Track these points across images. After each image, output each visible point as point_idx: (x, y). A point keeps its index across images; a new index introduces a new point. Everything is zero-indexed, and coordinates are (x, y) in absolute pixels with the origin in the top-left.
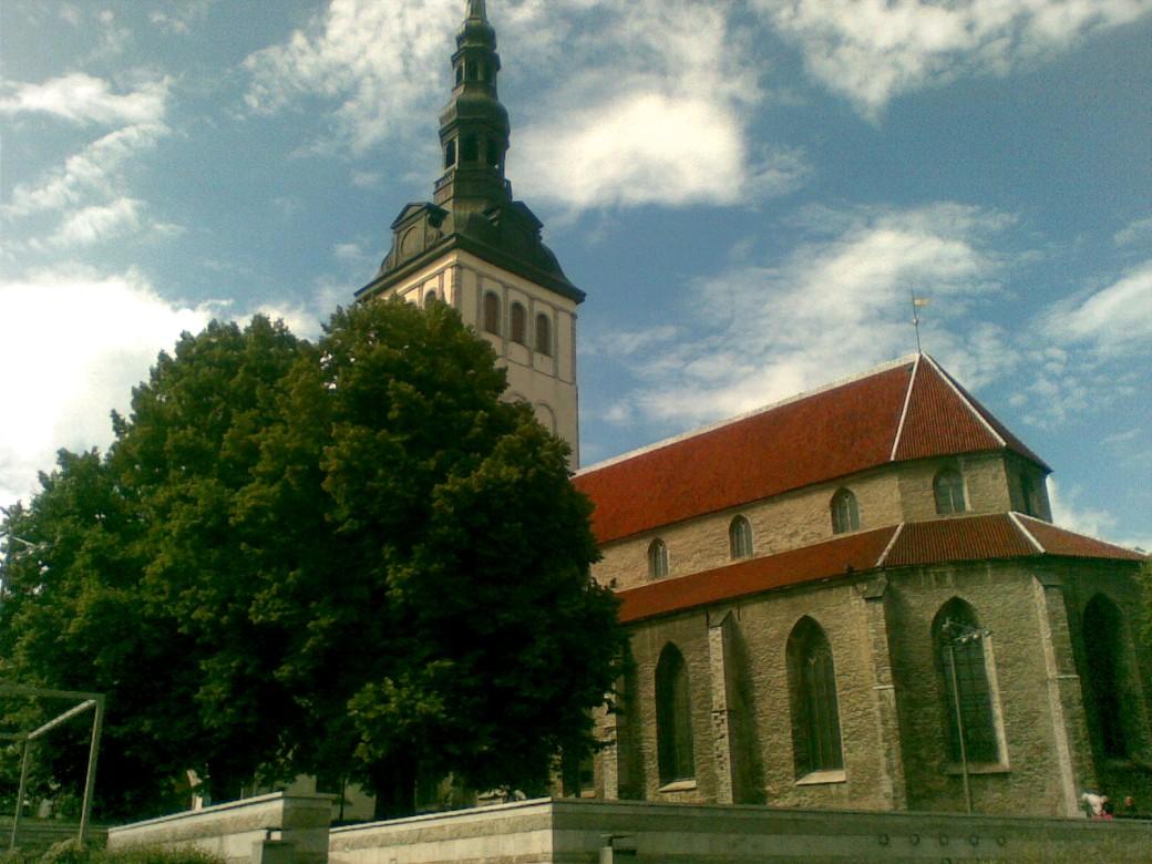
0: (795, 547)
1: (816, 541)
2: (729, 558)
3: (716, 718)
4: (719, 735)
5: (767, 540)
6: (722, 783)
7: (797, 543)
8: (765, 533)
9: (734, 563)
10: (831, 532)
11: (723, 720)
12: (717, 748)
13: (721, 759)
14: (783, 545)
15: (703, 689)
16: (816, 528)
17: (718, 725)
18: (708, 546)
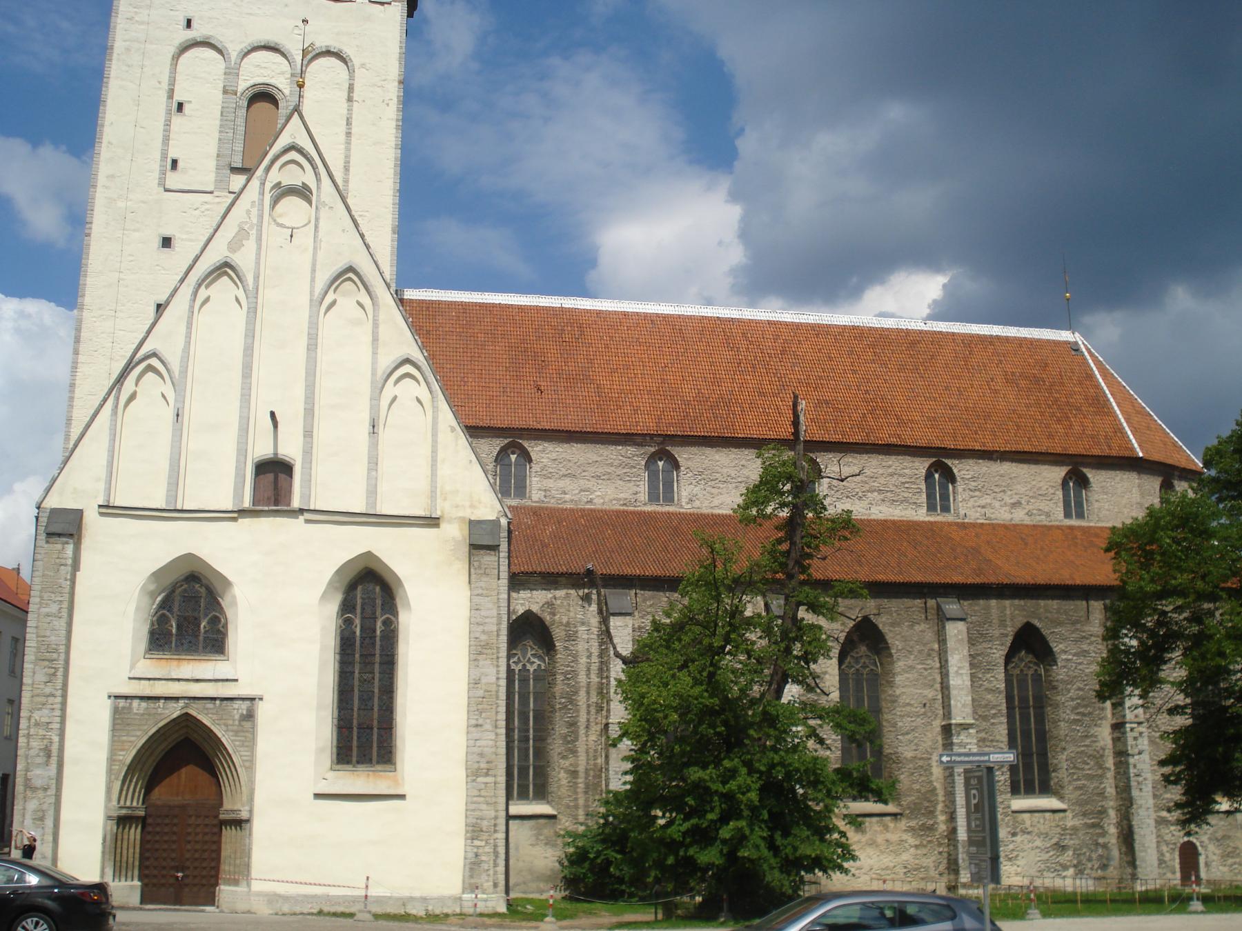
0: (1016, 521)
1: (1042, 520)
2: (924, 510)
3: (1132, 730)
4: (1136, 751)
5: (982, 502)
6: (1141, 807)
7: (1019, 516)
8: (977, 493)
9: (927, 519)
10: (1063, 515)
11: (1141, 734)
12: (1135, 766)
13: (1140, 779)
14: (1003, 515)
15: (1079, 689)
16: (1044, 506)
17: (1135, 739)
18: (893, 488)
